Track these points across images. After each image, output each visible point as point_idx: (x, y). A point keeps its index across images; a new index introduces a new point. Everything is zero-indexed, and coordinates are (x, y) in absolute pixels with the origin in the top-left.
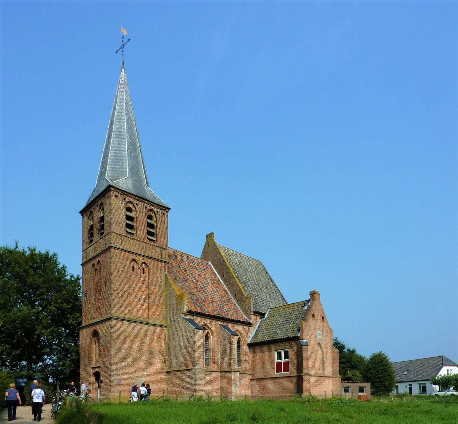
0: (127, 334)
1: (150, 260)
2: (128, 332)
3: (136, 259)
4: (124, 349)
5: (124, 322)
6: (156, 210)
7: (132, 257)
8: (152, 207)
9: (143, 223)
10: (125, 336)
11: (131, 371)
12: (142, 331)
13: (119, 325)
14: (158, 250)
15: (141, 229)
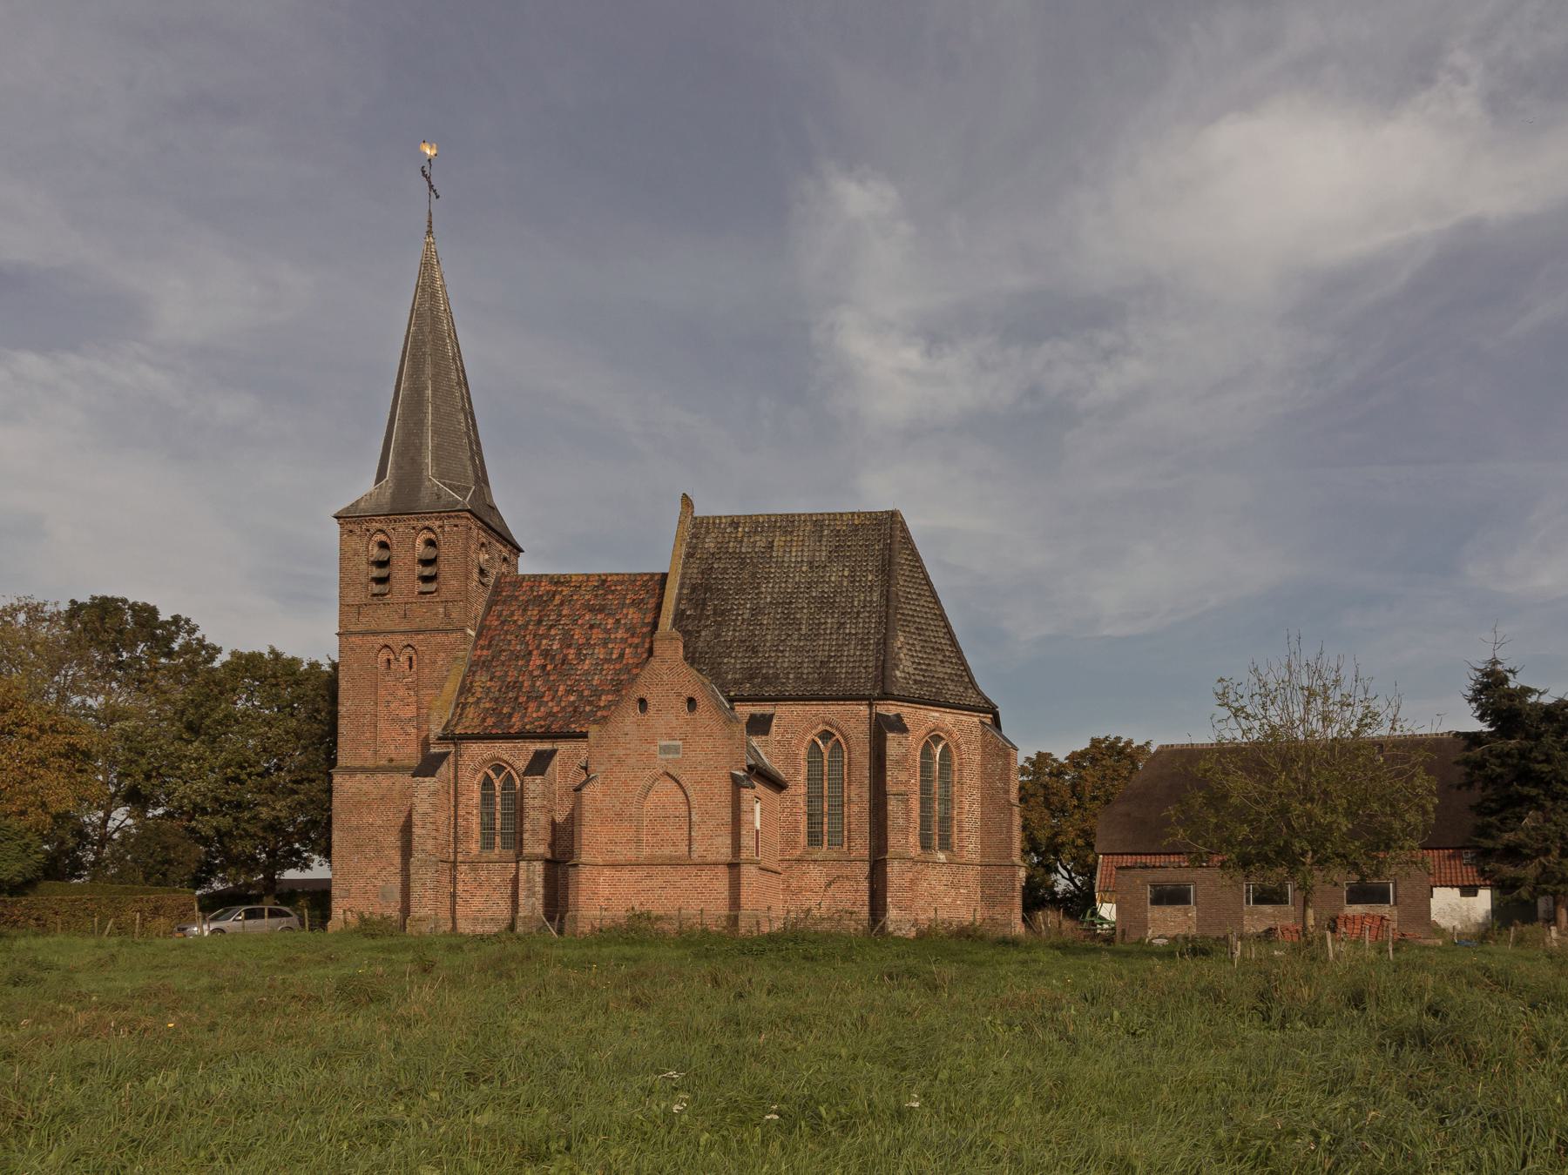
0: (364, 799)
1: (421, 637)
2: (366, 794)
3: (390, 643)
4: (358, 828)
5: (359, 776)
6: (435, 524)
7: (381, 640)
8: (427, 523)
9: (405, 564)
10: (359, 802)
11: (372, 871)
12: (398, 786)
13: (349, 784)
14: (441, 610)
15: (405, 573)
